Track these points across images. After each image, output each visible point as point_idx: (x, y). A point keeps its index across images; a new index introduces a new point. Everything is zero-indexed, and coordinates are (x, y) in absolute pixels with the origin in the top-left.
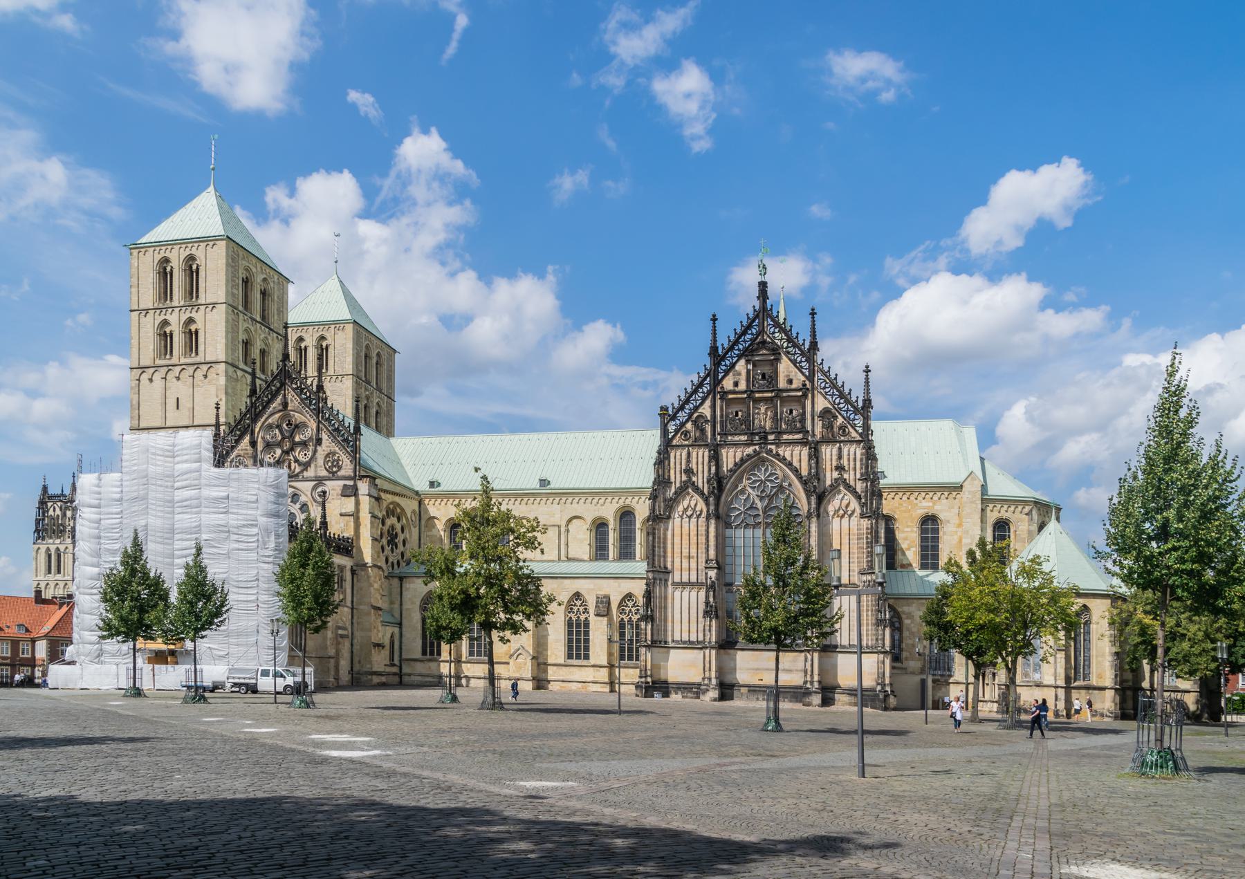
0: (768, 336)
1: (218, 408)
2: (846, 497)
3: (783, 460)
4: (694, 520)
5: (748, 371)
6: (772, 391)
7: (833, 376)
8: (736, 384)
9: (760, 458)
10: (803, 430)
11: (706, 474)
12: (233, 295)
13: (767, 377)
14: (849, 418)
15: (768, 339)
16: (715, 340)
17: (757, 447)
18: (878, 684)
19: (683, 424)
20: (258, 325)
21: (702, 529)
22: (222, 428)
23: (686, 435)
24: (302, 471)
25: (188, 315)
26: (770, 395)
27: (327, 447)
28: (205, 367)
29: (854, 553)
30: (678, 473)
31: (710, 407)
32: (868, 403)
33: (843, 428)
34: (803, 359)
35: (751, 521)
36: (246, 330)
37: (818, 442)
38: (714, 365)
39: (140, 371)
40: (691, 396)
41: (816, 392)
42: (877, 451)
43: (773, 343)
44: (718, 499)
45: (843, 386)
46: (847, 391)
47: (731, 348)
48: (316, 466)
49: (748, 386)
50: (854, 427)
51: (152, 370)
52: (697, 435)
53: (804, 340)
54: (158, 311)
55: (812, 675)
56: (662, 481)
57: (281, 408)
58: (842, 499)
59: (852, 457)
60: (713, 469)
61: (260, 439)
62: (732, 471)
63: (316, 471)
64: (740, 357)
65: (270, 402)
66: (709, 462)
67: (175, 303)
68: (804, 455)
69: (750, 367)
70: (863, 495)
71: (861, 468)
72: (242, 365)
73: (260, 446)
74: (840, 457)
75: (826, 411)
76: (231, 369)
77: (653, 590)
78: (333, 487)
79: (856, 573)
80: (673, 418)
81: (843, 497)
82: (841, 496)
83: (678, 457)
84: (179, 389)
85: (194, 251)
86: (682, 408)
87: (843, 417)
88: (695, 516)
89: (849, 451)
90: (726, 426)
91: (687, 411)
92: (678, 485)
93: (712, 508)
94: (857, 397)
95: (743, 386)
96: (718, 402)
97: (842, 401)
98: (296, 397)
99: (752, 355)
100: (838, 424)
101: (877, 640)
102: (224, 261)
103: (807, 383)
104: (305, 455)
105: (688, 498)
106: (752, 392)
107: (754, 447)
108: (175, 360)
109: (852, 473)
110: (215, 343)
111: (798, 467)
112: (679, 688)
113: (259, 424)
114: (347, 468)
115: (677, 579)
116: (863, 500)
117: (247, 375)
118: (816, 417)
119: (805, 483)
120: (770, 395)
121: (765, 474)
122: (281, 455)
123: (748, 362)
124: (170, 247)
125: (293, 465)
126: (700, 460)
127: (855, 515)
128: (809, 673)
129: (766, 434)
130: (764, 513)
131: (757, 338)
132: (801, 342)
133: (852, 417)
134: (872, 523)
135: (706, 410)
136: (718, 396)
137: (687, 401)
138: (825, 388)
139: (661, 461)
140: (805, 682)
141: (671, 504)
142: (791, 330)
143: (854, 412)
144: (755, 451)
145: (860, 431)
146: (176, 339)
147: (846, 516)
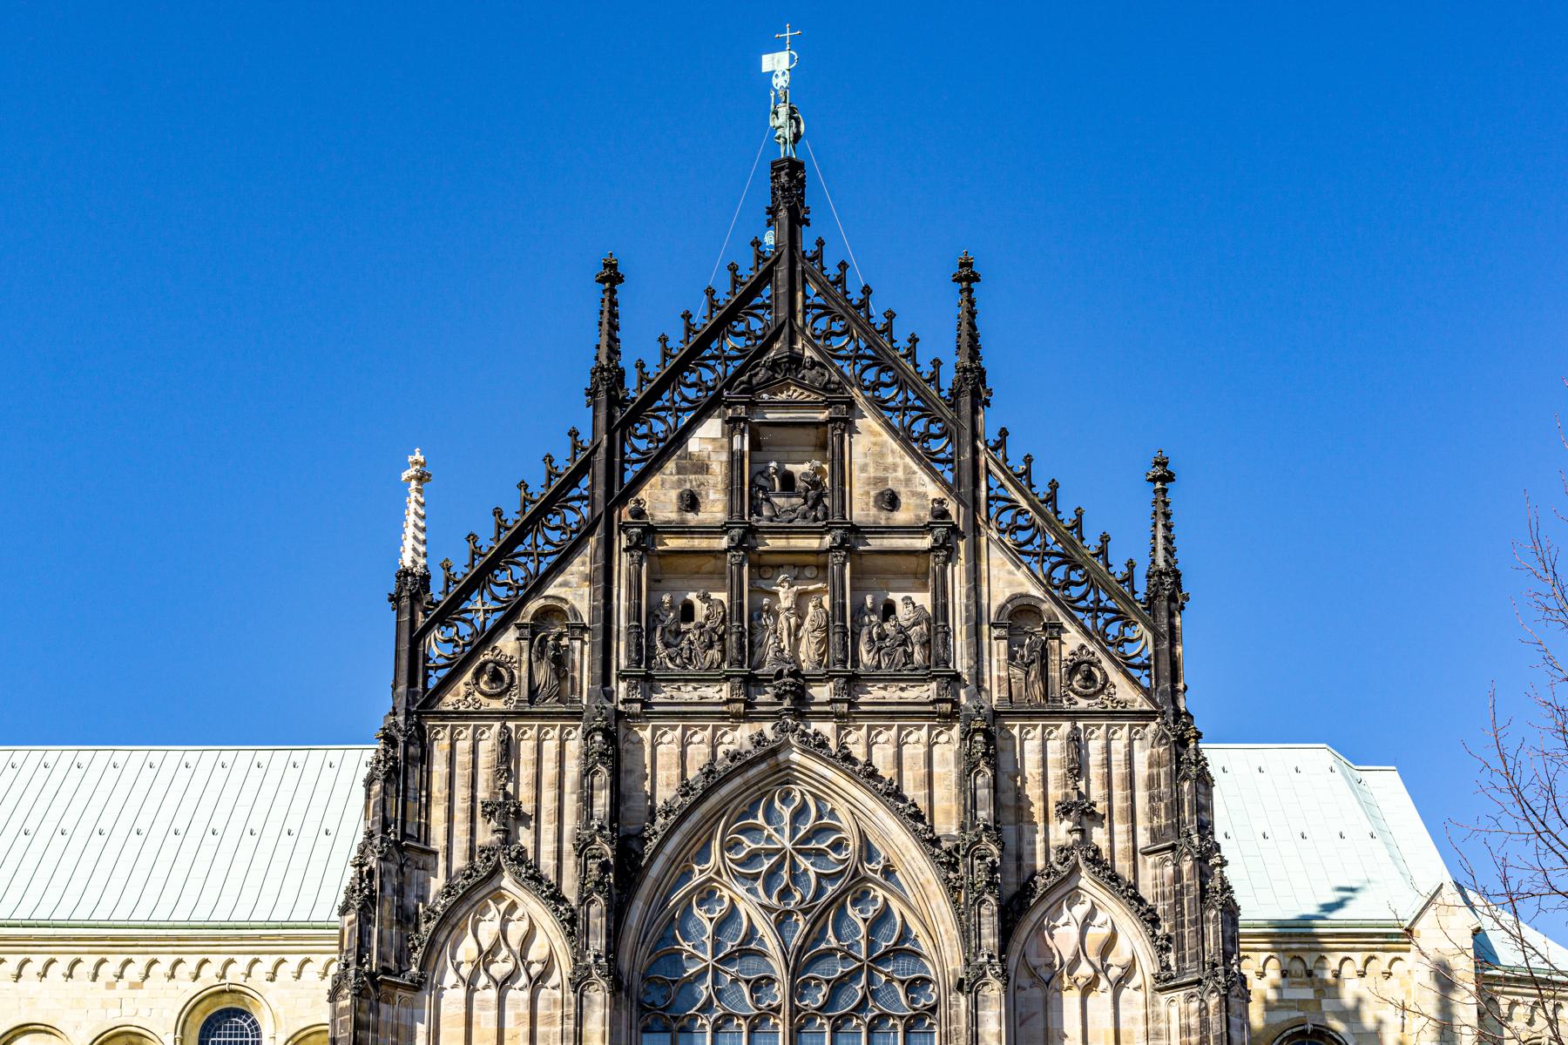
2: (1101, 917)
4: (518, 996)
5: (735, 460)
6: (821, 534)
7: (1042, 490)
8: (691, 502)
9: (777, 769)
10: (939, 669)
11: (570, 823)
13: (800, 484)
14: (1104, 635)
15: (808, 353)
17: (767, 727)
19: (488, 638)
23: (496, 677)
26: (813, 543)
30: (460, 816)
31: (590, 579)
33: (1080, 667)
37: (996, 715)
38: (610, 433)
40: (518, 537)
46: (1092, 542)
47: (671, 379)
50: (1125, 665)
53: (937, 363)
58: (1085, 926)
59: (1118, 771)
60: (602, 801)
66: (588, 772)
68: (945, 761)
69: (742, 443)
70: (1161, 908)
71: (1154, 812)
75: (1020, 613)
80: (447, 614)
81: (1091, 915)
82: (1080, 911)
83: (463, 758)
87: (1086, 632)
88: (523, 980)
89: (1108, 749)
90: (651, 647)
91: (502, 593)
92: (459, 862)
93: (597, 943)
94: (1131, 565)
95: (714, 509)
96: (623, 563)
97: (1074, 576)
100: (1065, 654)
103: (951, 507)
105: (494, 912)
106: (751, 531)
107: (756, 727)
109: (1120, 828)
111: (922, 805)
116: (1165, 927)
118: (985, 627)
119: (947, 861)
120: (813, 543)
121: (794, 831)
127: (1137, 980)
130: (794, 974)
131: (766, 347)
132: (926, 369)
137: (504, 554)
139: (394, 769)
142: (888, 329)
143: (1119, 616)
144: (759, 740)
145: (1145, 682)
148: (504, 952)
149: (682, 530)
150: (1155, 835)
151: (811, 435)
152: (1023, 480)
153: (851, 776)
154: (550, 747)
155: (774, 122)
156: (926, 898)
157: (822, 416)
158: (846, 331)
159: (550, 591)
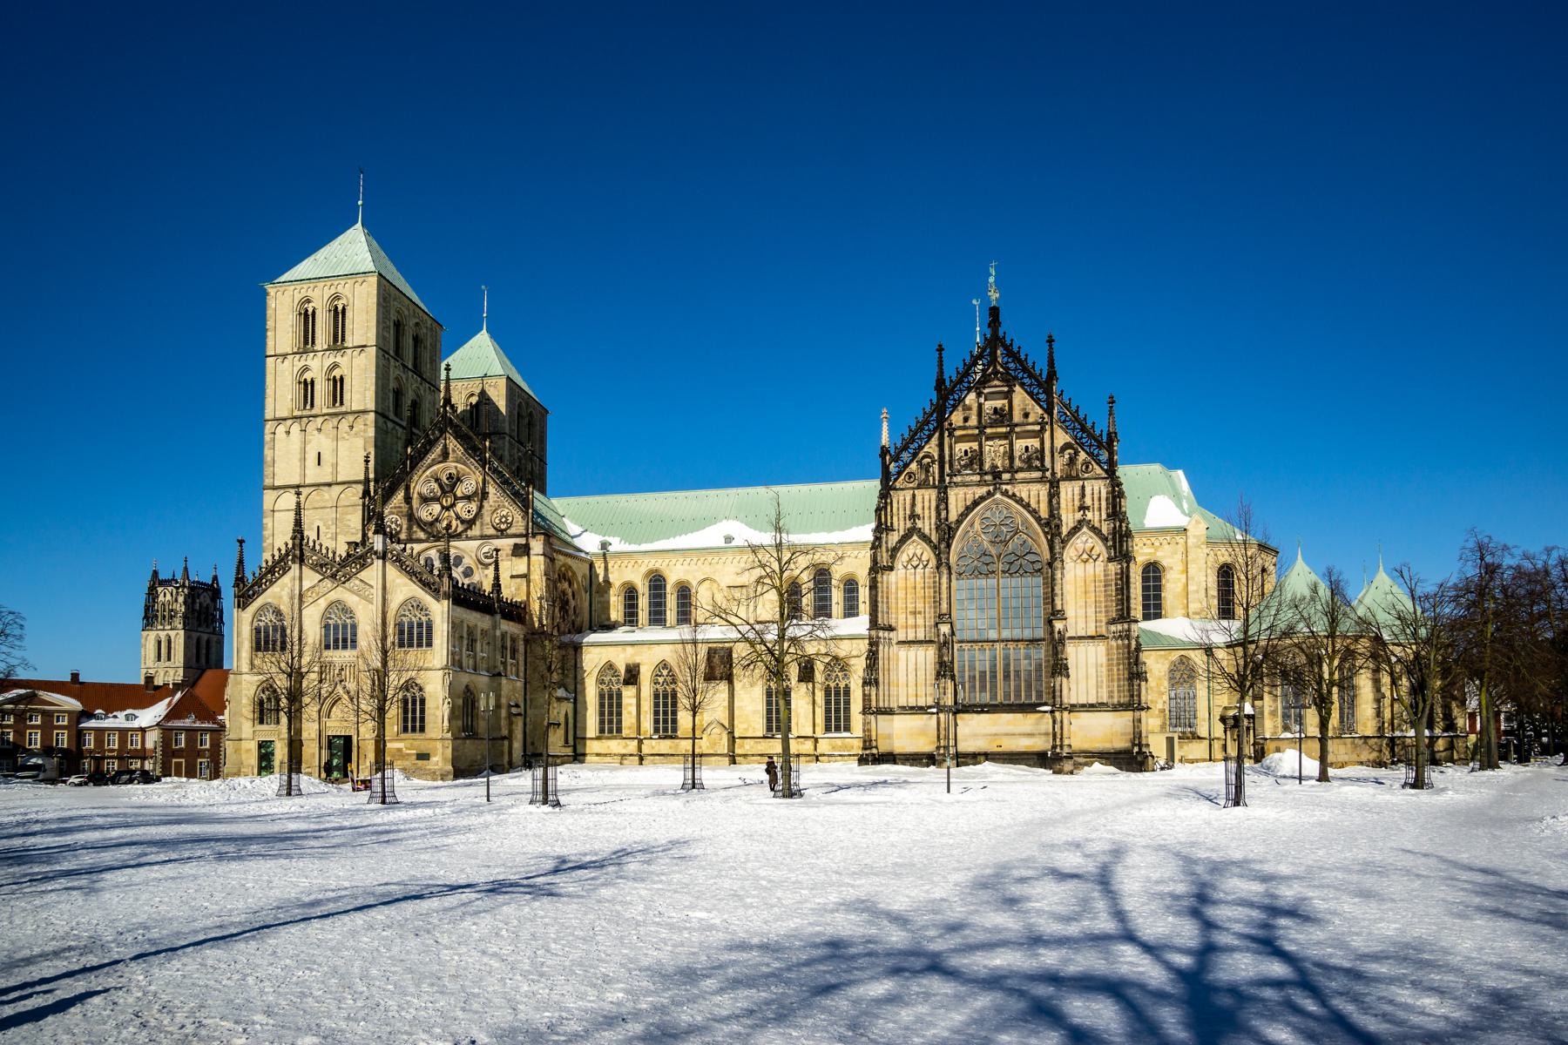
0: (1002, 367)
1: (367, 462)
2: (1090, 540)
3: (1020, 501)
5: (980, 406)
7: (1074, 408)
8: (966, 419)
10: (1043, 469)
12: (384, 338)
16: (941, 372)
17: (991, 488)
18: (1134, 745)
19: (906, 465)
20: (410, 373)
21: (930, 582)
22: (372, 484)
24: (466, 530)
25: (332, 359)
26: (1003, 430)
27: (495, 502)
28: (351, 418)
29: (1101, 602)
32: (1112, 437)
33: (1087, 464)
34: (1041, 391)
35: (984, 569)
36: (397, 378)
39: (276, 423)
40: (916, 434)
41: (1055, 426)
42: (1124, 487)
43: (1008, 373)
44: (949, 546)
45: (1085, 419)
47: (960, 381)
48: (482, 524)
49: (980, 421)
51: (289, 422)
52: (923, 477)
54: (298, 356)
55: (1061, 739)
56: (882, 529)
57: (441, 459)
59: (1096, 496)
61: (415, 495)
62: (963, 515)
63: (482, 530)
64: (969, 390)
65: (427, 452)
67: (318, 347)
69: (982, 400)
71: (1108, 508)
72: (392, 416)
73: (415, 502)
74: (1083, 495)
75: (1066, 446)
76: (381, 420)
77: (877, 650)
78: (506, 544)
79: (1104, 624)
80: (896, 458)
82: (1084, 539)
83: (901, 502)
84: (320, 442)
85: (340, 289)
86: (905, 448)
88: (921, 566)
91: (911, 451)
92: (902, 533)
95: (973, 421)
96: (947, 440)
98: (458, 446)
99: (984, 388)
101: (1132, 696)
102: (375, 300)
104: (469, 511)
108: (315, 411)
109: (1097, 513)
110: (362, 392)
112: (907, 760)
113: (415, 478)
114: (519, 525)
115: (902, 637)
117: (397, 427)
118: (1056, 454)
120: (1003, 430)
122: (441, 512)
123: (979, 395)
124: (312, 285)
125: (454, 523)
126: (927, 504)
127: (1101, 558)
128: (1059, 736)
129: (1001, 473)
132: (1038, 372)
133: (1096, 452)
134: (1122, 568)
135: (932, 448)
136: (946, 434)
137: (912, 440)
138: (1065, 421)
140: (1054, 747)
141: (894, 552)
142: (1026, 359)
146: (317, 387)
147: (1091, 560)
148: (915, 558)
149: (964, 428)
150: (1108, 515)
151: (1002, 395)
152: (1068, 407)
153: (1017, 502)
154: (927, 497)
155: (990, 294)
156: (1039, 537)
157: (1006, 389)
158: (1013, 361)
159: (926, 449)
